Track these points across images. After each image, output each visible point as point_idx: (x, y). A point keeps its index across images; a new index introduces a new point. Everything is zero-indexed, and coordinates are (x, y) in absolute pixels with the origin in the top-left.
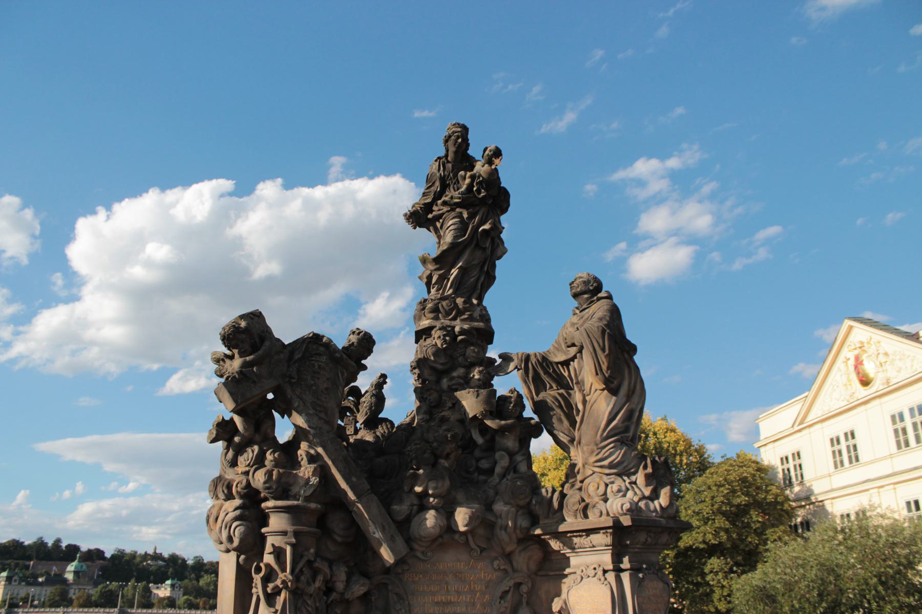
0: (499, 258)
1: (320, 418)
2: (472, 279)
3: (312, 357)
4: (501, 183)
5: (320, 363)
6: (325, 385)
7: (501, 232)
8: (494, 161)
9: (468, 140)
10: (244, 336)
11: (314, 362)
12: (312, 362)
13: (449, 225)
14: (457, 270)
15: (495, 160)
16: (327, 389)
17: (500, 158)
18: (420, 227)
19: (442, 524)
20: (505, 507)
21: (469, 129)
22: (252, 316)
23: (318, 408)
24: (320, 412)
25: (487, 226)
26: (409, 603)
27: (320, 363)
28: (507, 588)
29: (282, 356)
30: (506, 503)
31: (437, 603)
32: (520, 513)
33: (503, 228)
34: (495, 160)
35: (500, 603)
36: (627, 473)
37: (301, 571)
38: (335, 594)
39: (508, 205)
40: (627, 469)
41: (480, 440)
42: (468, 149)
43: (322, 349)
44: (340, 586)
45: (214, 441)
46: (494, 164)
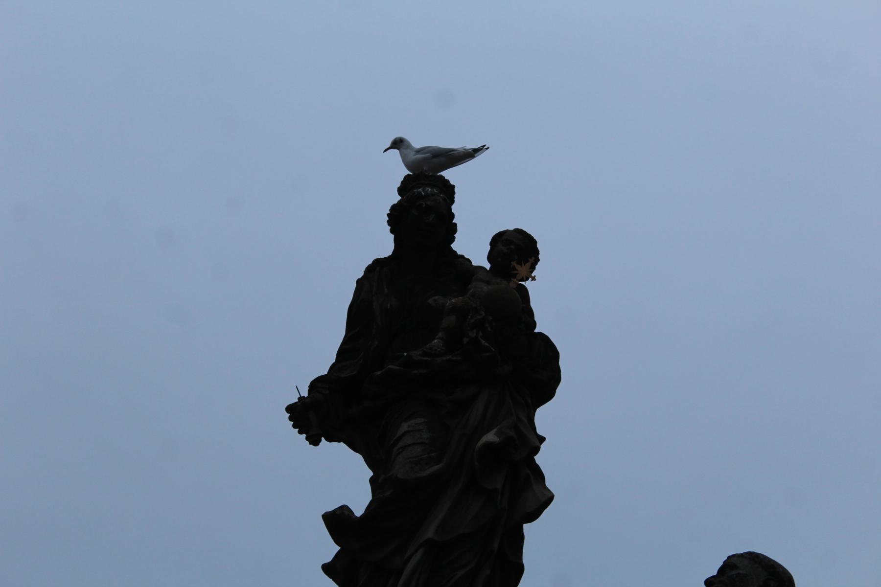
0: (533, 516)
2: (461, 573)
4: (534, 324)
7: (537, 450)
8: (515, 269)
9: (452, 216)
13: (399, 434)
14: (421, 551)
15: (518, 267)
17: (532, 260)
18: (330, 440)
21: (456, 190)
25: (491, 437)
33: (542, 439)
34: (518, 267)
39: (556, 378)
42: (453, 240)
46: (515, 276)
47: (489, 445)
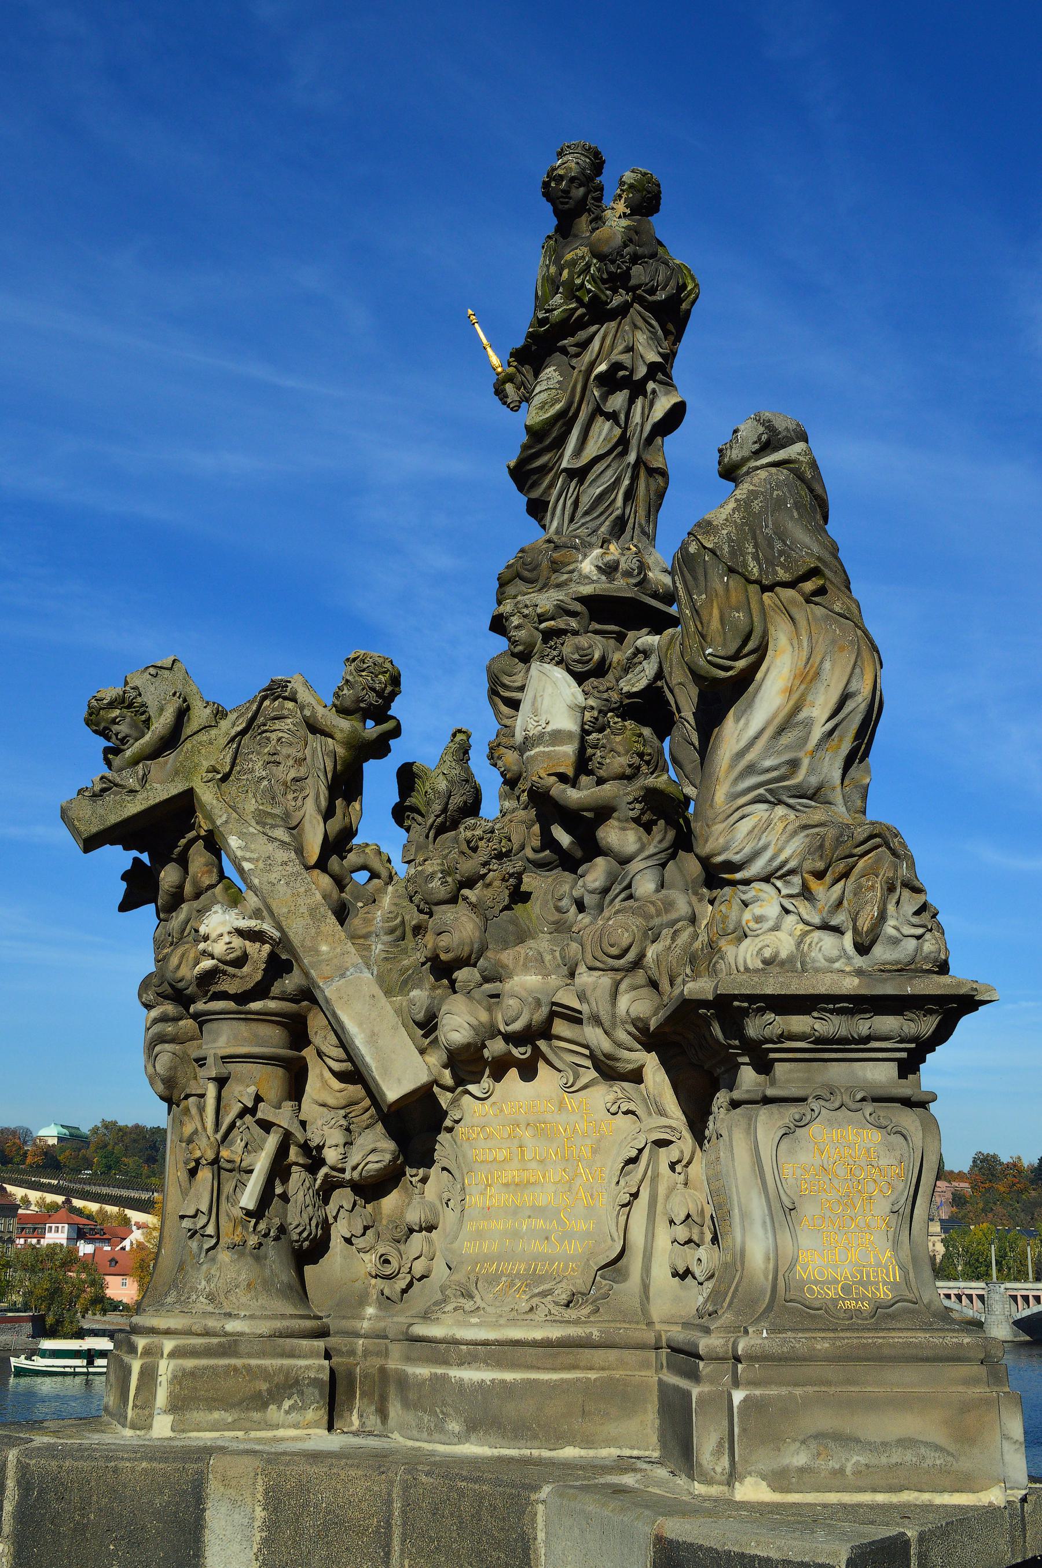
1: (272, 839)
3: (265, 725)
5: (281, 734)
6: (292, 774)
10: (116, 712)
11: (268, 734)
12: (264, 735)
16: (296, 780)
19: (475, 1022)
20: (590, 976)
22: (152, 671)
23: (269, 821)
24: (273, 826)
25: (603, 367)
26: (463, 1189)
27: (281, 734)
28: (634, 1153)
29: (213, 732)
30: (590, 969)
31: (507, 1185)
32: (623, 986)
35: (618, 1183)
36: (776, 875)
37: (232, 1126)
38: (324, 1170)
40: (776, 863)
41: (564, 839)
43: (290, 705)
44: (331, 1156)
45: (124, 907)
47: (600, 377)
